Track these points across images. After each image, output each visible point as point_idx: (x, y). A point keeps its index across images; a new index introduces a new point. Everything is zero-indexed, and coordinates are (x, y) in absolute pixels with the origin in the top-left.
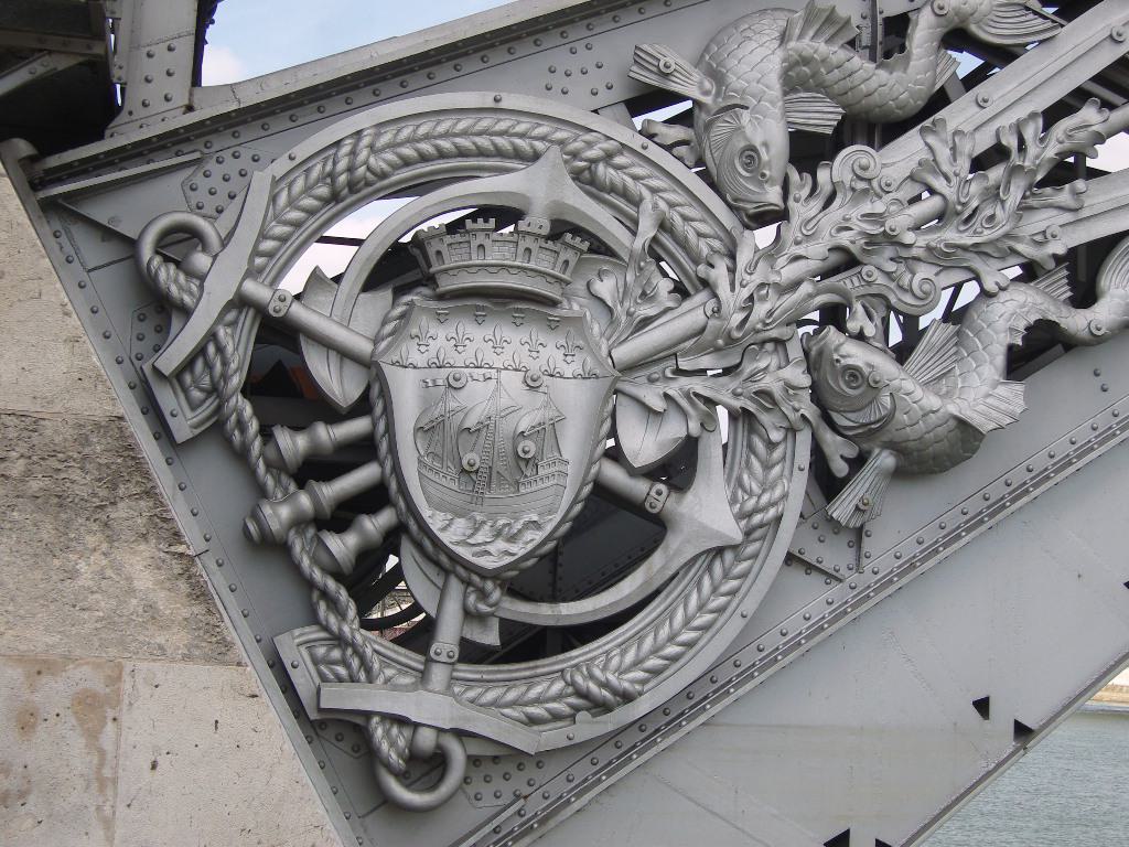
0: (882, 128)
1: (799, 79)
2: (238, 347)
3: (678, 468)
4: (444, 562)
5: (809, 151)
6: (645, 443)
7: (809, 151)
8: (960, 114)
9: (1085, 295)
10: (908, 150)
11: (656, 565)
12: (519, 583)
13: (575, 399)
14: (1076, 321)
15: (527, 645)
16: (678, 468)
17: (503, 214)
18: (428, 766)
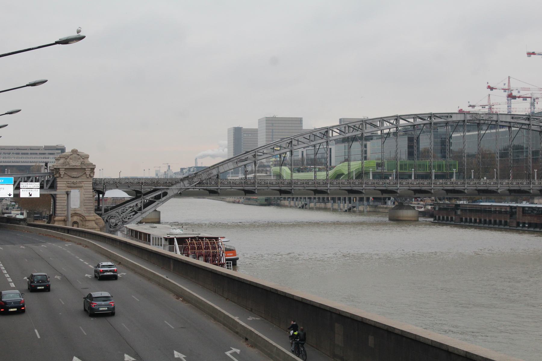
0: (123, 212)
1: (121, 211)
2: (106, 220)
3: (118, 223)
4: (112, 226)
5: (122, 213)
6: (117, 222)
7: (122, 213)
8: (126, 212)
9: (130, 217)
10: (125, 213)
11: (118, 225)
12: (114, 226)
13: (115, 221)
14: (130, 218)
15: (114, 228)
16: (118, 223)
17: (113, 216)
18: (112, 231)
